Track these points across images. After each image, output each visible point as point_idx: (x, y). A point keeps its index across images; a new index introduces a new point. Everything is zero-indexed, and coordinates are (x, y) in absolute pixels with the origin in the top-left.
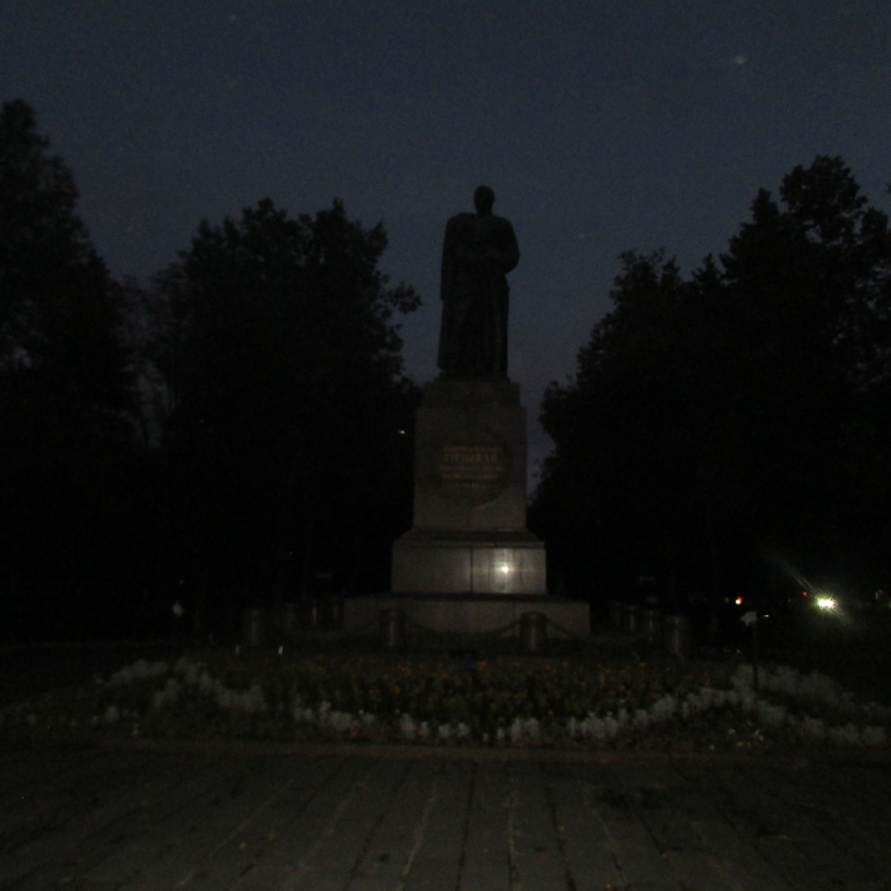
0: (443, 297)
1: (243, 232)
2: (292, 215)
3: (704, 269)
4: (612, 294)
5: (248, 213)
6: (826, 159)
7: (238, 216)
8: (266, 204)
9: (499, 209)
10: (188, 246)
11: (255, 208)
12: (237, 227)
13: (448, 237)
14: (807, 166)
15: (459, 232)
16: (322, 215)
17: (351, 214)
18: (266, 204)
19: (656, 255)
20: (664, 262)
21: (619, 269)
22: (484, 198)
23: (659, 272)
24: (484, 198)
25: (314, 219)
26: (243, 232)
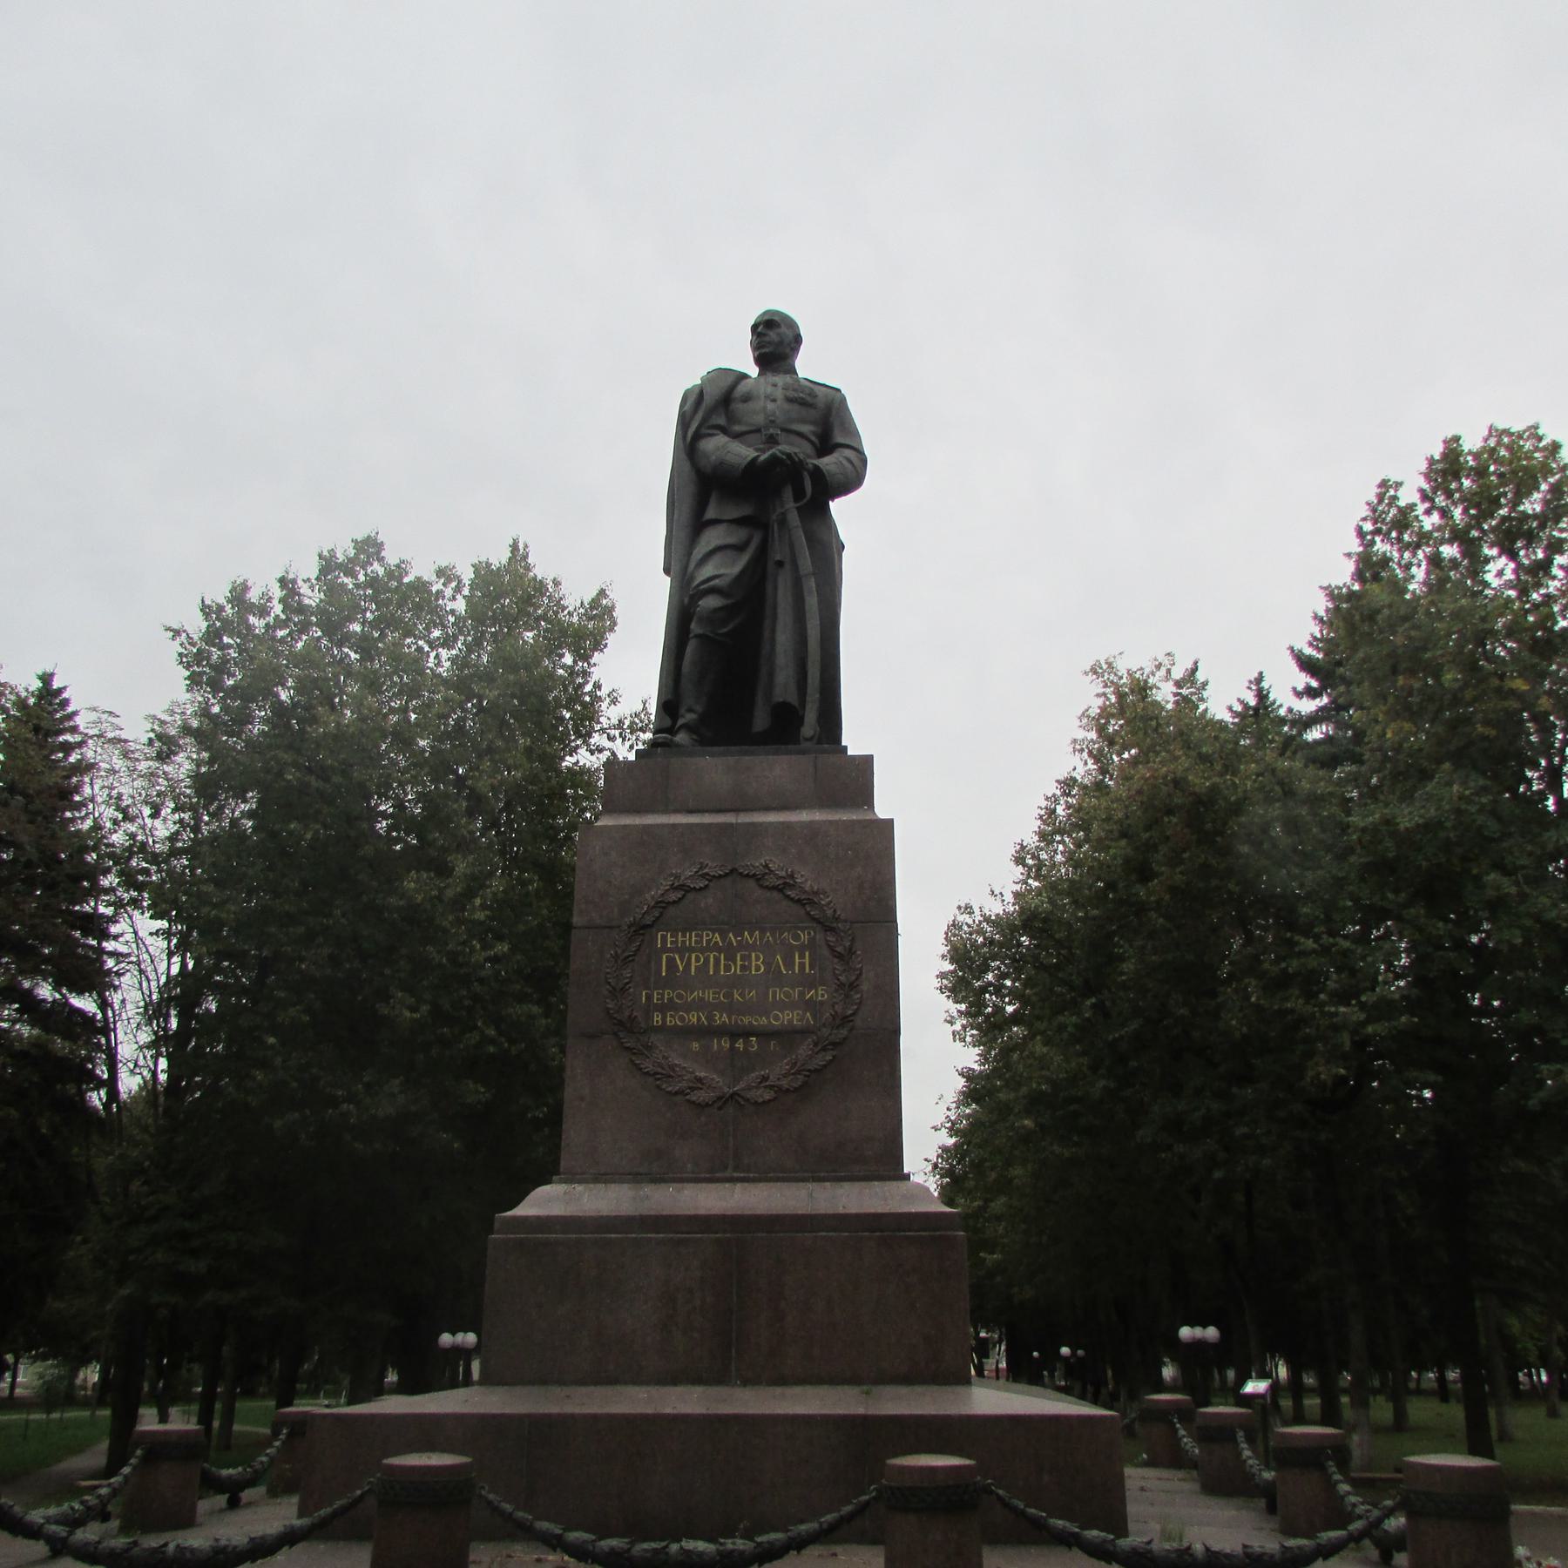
0: (667, 571)
1: (312, 597)
2: (421, 569)
3: (1253, 702)
4: (1077, 746)
5: (328, 565)
6: (1506, 432)
7: (307, 569)
8: (369, 548)
9: (807, 366)
10: (197, 625)
11: (345, 550)
12: (304, 589)
13: (684, 421)
14: (1472, 442)
15: (710, 410)
16: (486, 576)
17: (542, 568)
18: (369, 548)
19: (1159, 667)
20: (1178, 674)
21: (1091, 697)
22: (775, 340)
23: (1165, 694)
24: (775, 340)
25: (467, 575)
26: (312, 597)
